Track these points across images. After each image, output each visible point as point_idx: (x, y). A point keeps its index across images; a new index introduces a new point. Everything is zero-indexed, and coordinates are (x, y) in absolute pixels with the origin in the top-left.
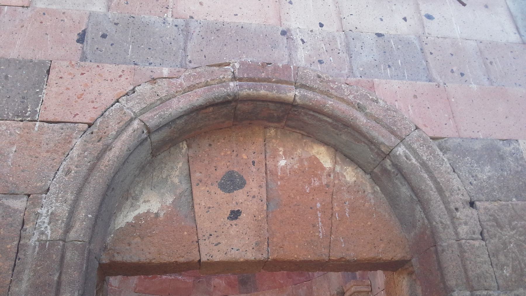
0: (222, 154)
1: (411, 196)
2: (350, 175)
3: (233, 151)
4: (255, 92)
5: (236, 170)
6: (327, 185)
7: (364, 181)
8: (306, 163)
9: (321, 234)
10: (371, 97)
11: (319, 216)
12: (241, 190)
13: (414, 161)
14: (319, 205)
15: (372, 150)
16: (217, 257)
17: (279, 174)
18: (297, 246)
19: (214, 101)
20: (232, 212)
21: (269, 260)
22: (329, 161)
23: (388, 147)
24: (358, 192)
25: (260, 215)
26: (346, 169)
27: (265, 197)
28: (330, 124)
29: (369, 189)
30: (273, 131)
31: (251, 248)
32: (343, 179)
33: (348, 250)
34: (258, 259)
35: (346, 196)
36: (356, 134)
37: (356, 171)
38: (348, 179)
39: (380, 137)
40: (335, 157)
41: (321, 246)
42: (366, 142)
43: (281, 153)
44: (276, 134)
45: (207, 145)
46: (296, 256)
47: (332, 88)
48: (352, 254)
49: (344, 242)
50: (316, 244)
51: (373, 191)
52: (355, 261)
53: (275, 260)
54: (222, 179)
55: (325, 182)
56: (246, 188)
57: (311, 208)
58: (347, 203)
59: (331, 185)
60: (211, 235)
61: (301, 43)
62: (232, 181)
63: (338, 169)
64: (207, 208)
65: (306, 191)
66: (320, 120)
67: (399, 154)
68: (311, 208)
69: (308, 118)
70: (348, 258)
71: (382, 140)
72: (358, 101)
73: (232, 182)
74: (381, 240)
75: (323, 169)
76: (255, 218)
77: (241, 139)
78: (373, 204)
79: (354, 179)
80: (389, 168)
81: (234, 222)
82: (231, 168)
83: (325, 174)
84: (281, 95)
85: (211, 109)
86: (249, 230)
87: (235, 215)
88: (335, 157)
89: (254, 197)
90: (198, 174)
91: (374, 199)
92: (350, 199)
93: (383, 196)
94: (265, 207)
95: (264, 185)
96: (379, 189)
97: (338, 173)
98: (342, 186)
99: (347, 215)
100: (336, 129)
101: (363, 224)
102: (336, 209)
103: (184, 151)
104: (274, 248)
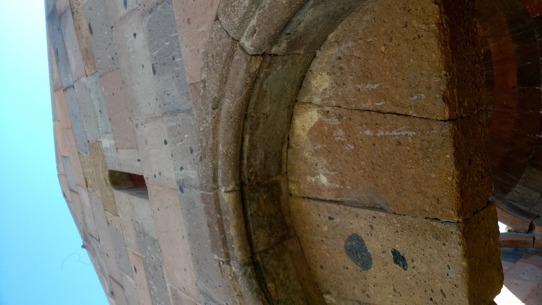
0: (328, 255)
1: (312, 6)
2: (320, 82)
3: (322, 241)
4: (234, 242)
5: (343, 244)
6: (340, 117)
7: (326, 60)
8: (319, 146)
9: (410, 133)
10: (202, 91)
11: (382, 134)
12: (366, 243)
13: (254, 22)
14: (368, 132)
15: (267, 75)
16: (462, 299)
17: (337, 186)
18: (433, 176)
19: (256, 290)
20: (396, 261)
21: (461, 220)
22: (310, 113)
23: (249, 63)
24: (341, 68)
25: (394, 223)
26: (316, 88)
27: (369, 211)
28: (252, 134)
29: (334, 51)
30: (292, 187)
31: (444, 248)
32: (328, 92)
33: (429, 88)
34: (459, 240)
35: (350, 86)
36: (253, 100)
37: (315, 73)
38: (326, 85)
39: (239, 77)
40: (304, 103)
41: (428, 135)
42: (258, 85)
43: (313, 180)
44: (294, 182)
45: (322, 270)
46: (450, 178)
47: (207, 144)
48: (435, 80)
49: (417, 93)
50: (426, 144)
51: (336, 45)
52: (448, 69)
53: (460, 213)
54: (357, 264)
55: (335, 122)
56: (362, 235)
57: (374, 145)
58: (359, 87)
59: (338, 111)
60: (431, 299)
61: (183, 171)
62: (357, 253)
63: (317, 100)
64: (395, 294)
65: (353, 150)
66: (253, 146)
67: (251, 47)
68: (374, 145)
69: (255, 161)
70: (443, 87)
71: (242, 74)
72: (210, 109)
73: (358, 251)
74: (406, 26)
75: (320, 123)
76: (400, 232)
77: (307, 228)
78: (354, 44)
79: (325, 75)
80: (284, 45)
81: (409, 262)
82: (342, 249)
83: (327, 120)
84: (230, 210)
85: (270, 285)
86: (418, 245)
87: (399, 258)
88: (304, 103)
89: (371, 227)
90: (356, 291)
91: (346, 42)
92: (352, 81)
93: (339, 27)
94: (383, 214)
95: (354, 210)
96: (331, 35)
97: (323, 100)
98: (337, 94)
99: (375, 87)
100: (258, 123)
101: (385, 60)
102: (368, 105)
103: (334, 301)
104: (440, 212)
